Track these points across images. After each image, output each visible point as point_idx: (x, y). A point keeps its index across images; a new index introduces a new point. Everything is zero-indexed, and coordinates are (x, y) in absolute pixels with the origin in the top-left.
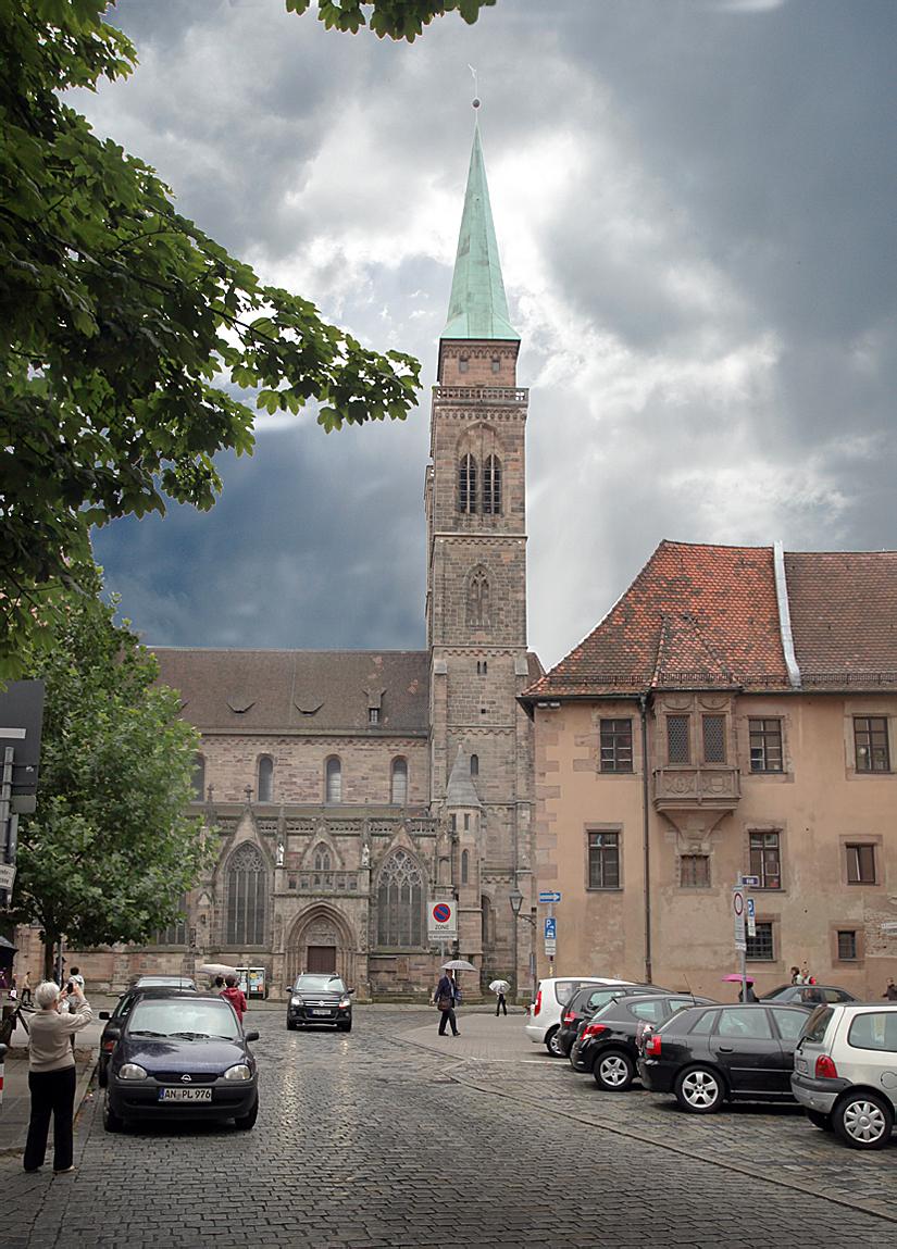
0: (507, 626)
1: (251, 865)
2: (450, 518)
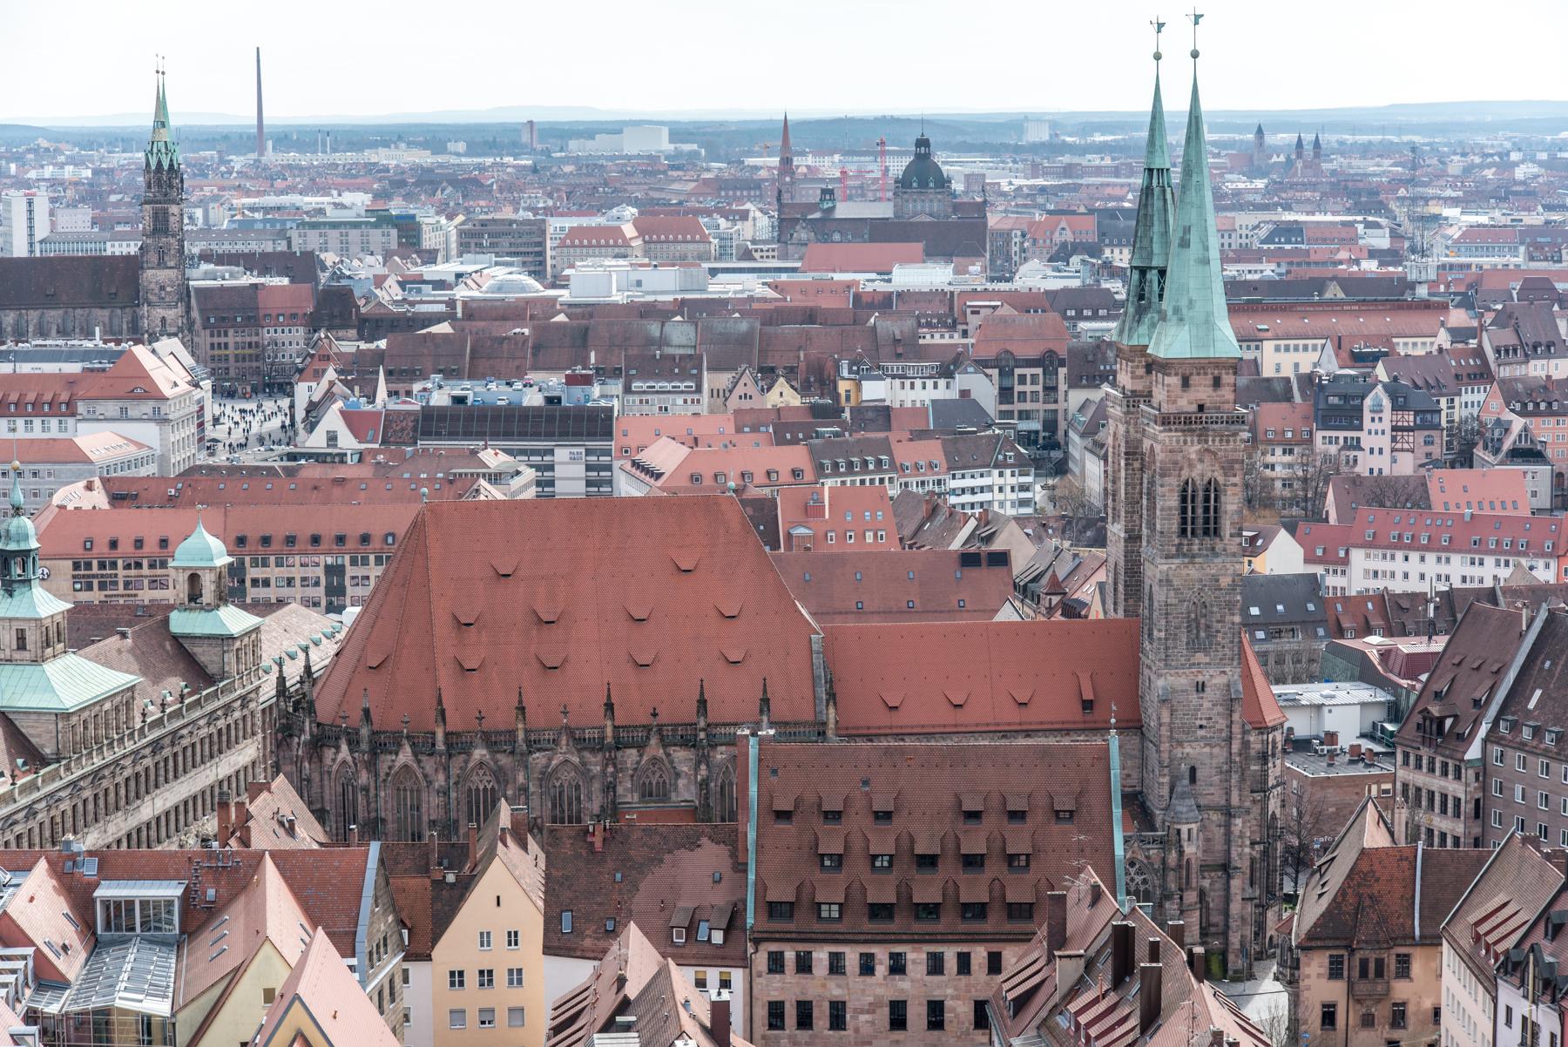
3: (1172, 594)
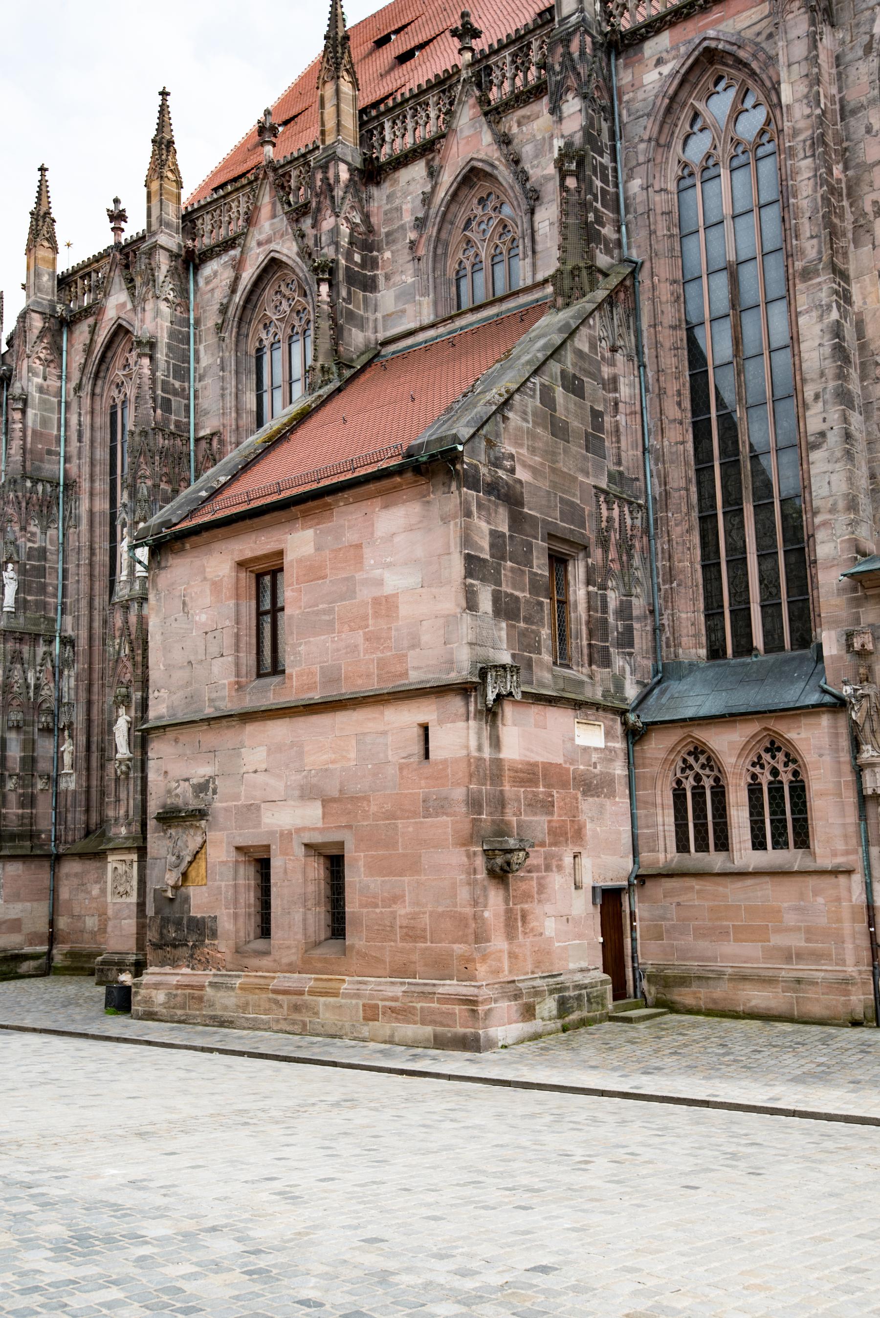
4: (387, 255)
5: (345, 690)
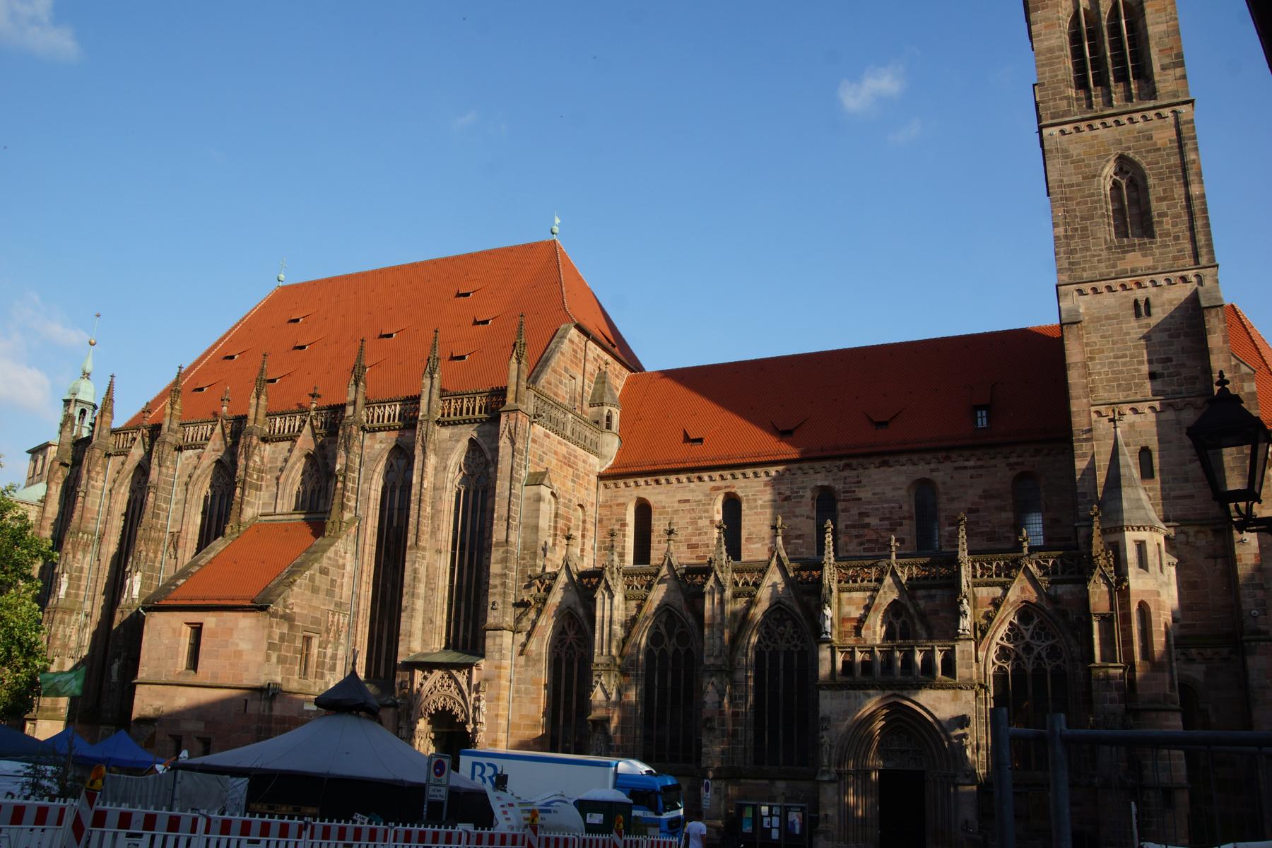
0: (1177, 238)
1: (788, 642)
2: (1061, 99)
3: (1070, 168)
4: (269, 477)
5: (219, 682)
